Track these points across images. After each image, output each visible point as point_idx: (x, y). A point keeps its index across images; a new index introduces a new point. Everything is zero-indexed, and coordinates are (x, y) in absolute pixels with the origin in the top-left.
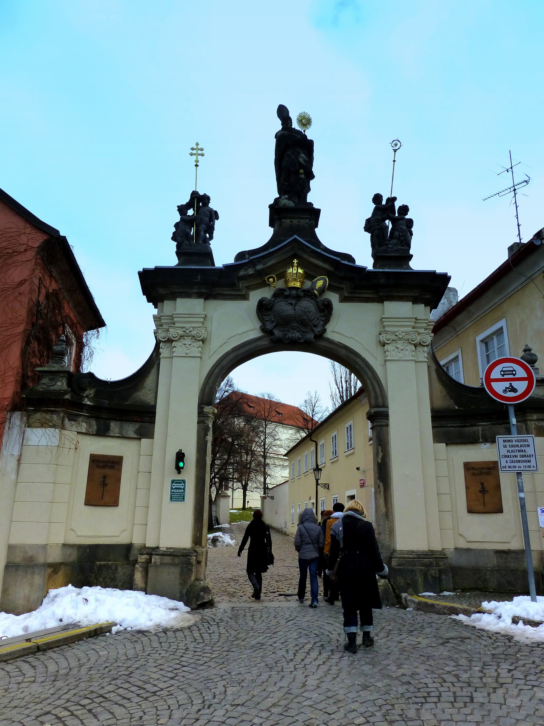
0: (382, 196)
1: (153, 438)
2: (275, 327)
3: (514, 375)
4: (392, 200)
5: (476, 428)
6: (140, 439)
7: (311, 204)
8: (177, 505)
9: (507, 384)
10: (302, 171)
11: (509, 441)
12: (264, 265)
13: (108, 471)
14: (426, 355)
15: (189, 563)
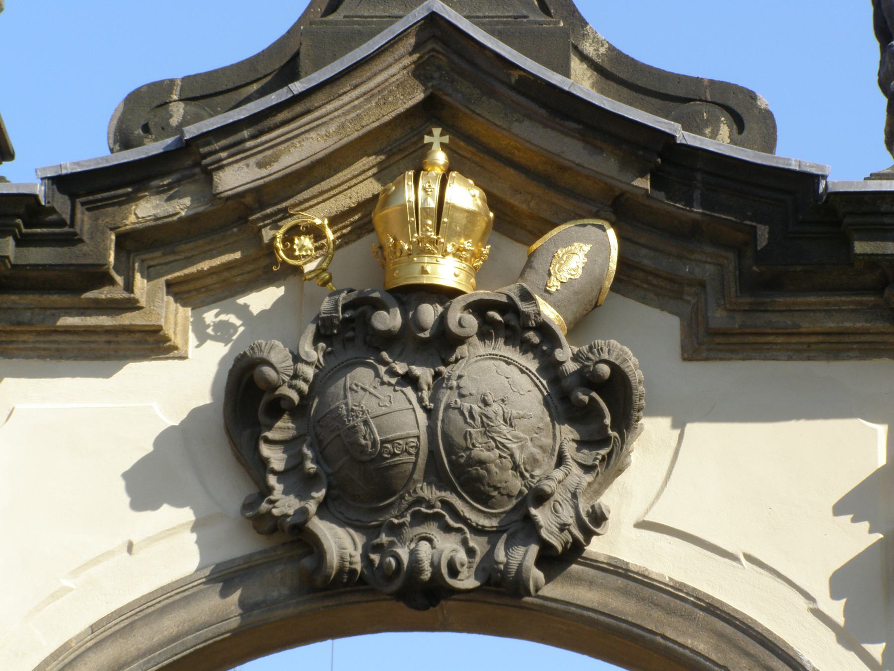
12: (260, 165)
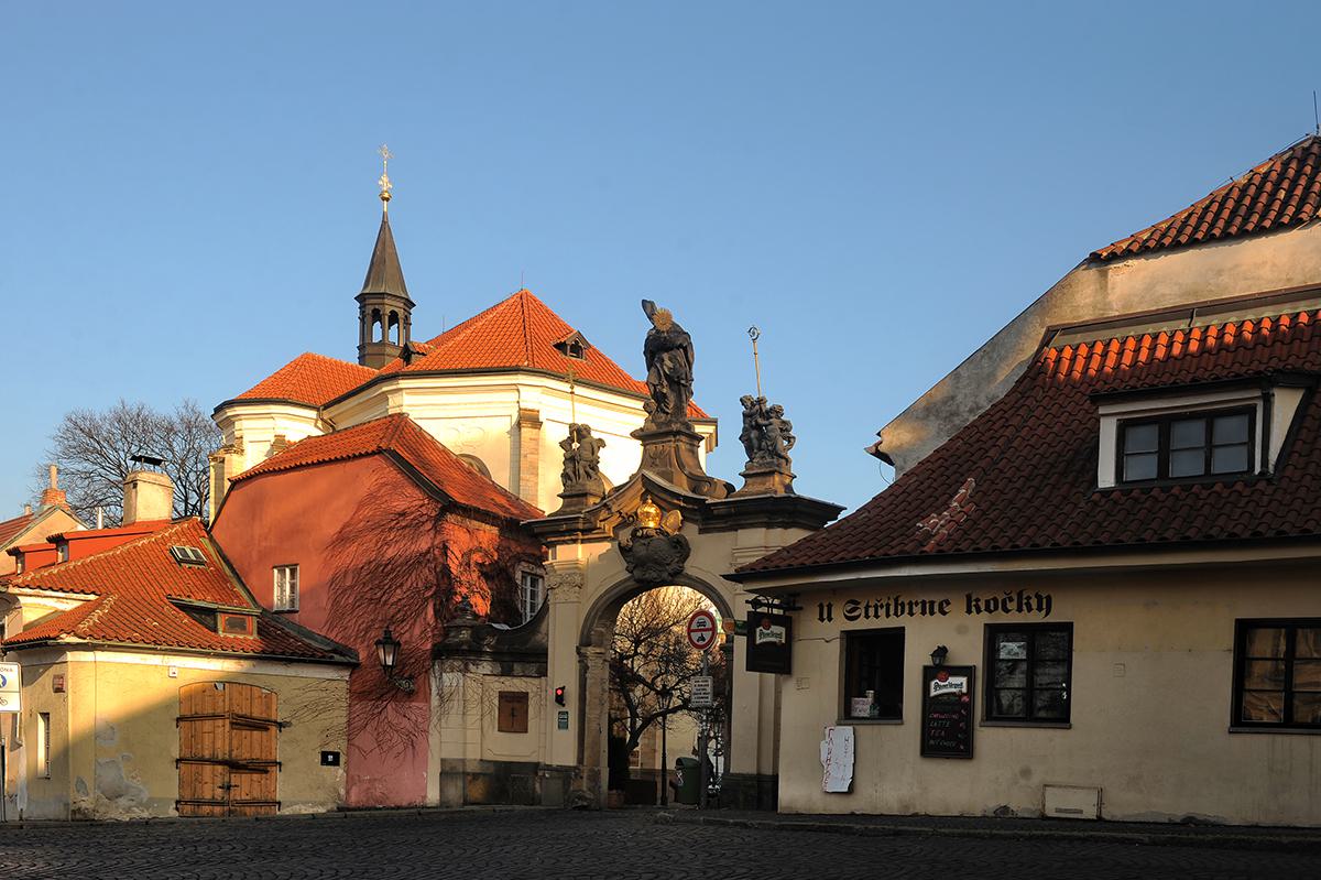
9: (699, 634)
13: (516, 705)
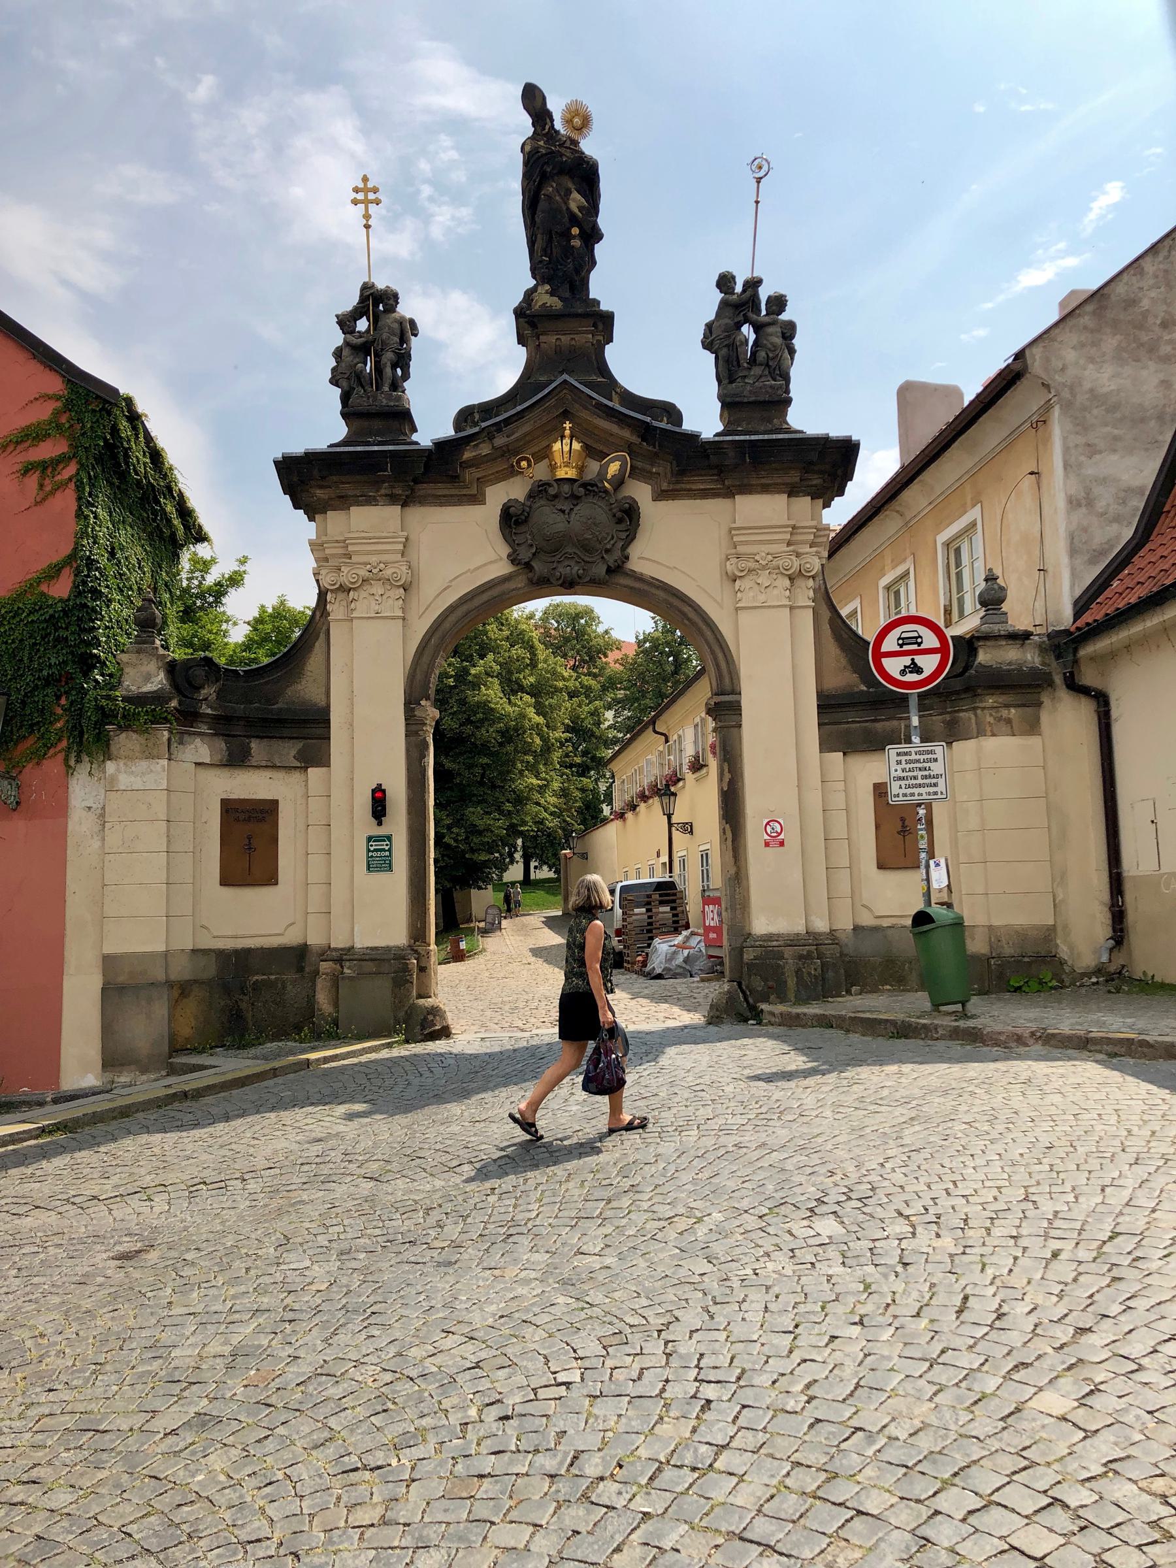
0: (733, 278)
1: (329, 766)
2: (534, 554)
3: (919, 644)
4: (753, 284)
5: (895, 723)
6: (305, 769)
7: (596, 303)
8: (382, 877)
9: (907, 661)
10: (575, 231)
11: (906, 754)
14: (811, 594)
15: (406, 969)
